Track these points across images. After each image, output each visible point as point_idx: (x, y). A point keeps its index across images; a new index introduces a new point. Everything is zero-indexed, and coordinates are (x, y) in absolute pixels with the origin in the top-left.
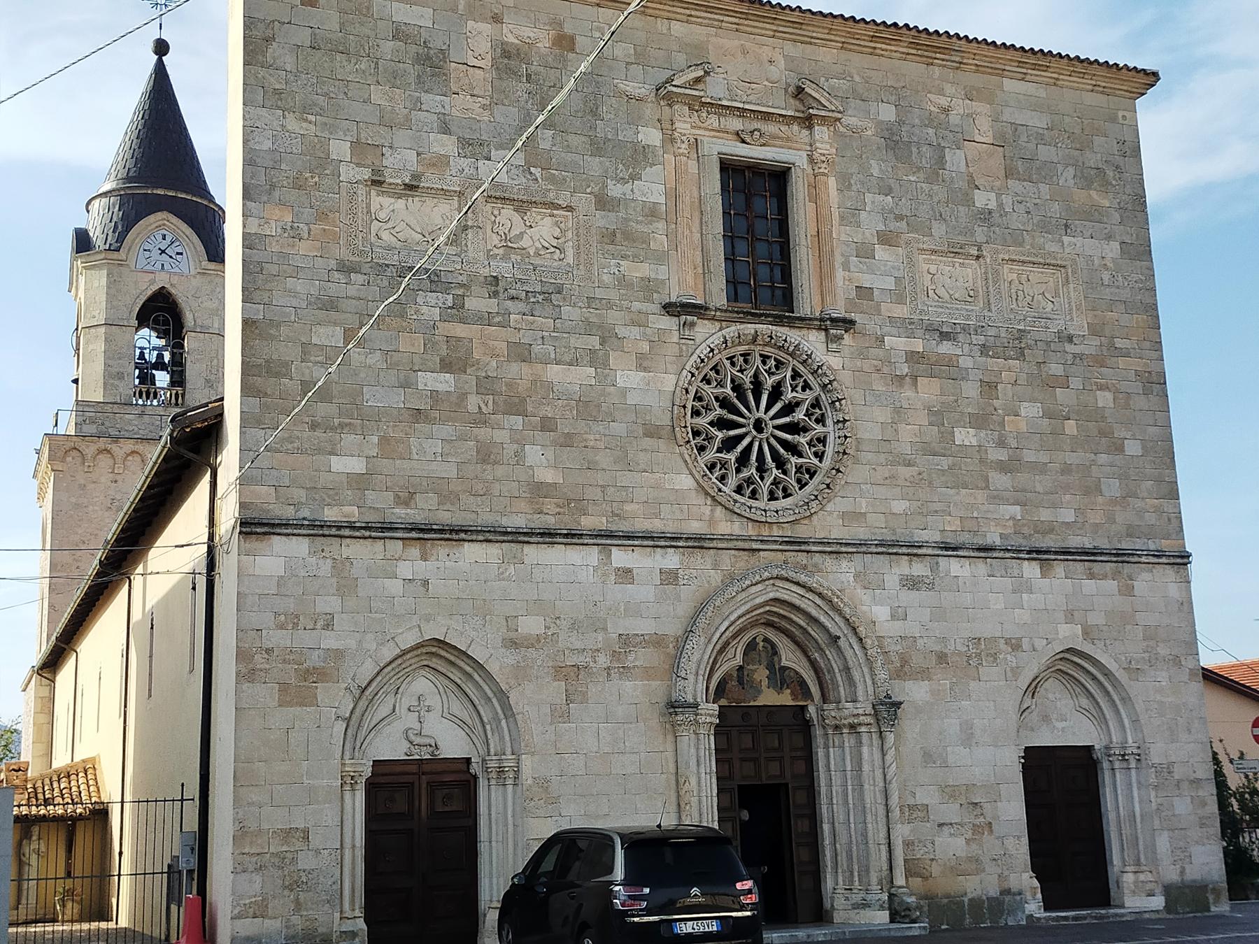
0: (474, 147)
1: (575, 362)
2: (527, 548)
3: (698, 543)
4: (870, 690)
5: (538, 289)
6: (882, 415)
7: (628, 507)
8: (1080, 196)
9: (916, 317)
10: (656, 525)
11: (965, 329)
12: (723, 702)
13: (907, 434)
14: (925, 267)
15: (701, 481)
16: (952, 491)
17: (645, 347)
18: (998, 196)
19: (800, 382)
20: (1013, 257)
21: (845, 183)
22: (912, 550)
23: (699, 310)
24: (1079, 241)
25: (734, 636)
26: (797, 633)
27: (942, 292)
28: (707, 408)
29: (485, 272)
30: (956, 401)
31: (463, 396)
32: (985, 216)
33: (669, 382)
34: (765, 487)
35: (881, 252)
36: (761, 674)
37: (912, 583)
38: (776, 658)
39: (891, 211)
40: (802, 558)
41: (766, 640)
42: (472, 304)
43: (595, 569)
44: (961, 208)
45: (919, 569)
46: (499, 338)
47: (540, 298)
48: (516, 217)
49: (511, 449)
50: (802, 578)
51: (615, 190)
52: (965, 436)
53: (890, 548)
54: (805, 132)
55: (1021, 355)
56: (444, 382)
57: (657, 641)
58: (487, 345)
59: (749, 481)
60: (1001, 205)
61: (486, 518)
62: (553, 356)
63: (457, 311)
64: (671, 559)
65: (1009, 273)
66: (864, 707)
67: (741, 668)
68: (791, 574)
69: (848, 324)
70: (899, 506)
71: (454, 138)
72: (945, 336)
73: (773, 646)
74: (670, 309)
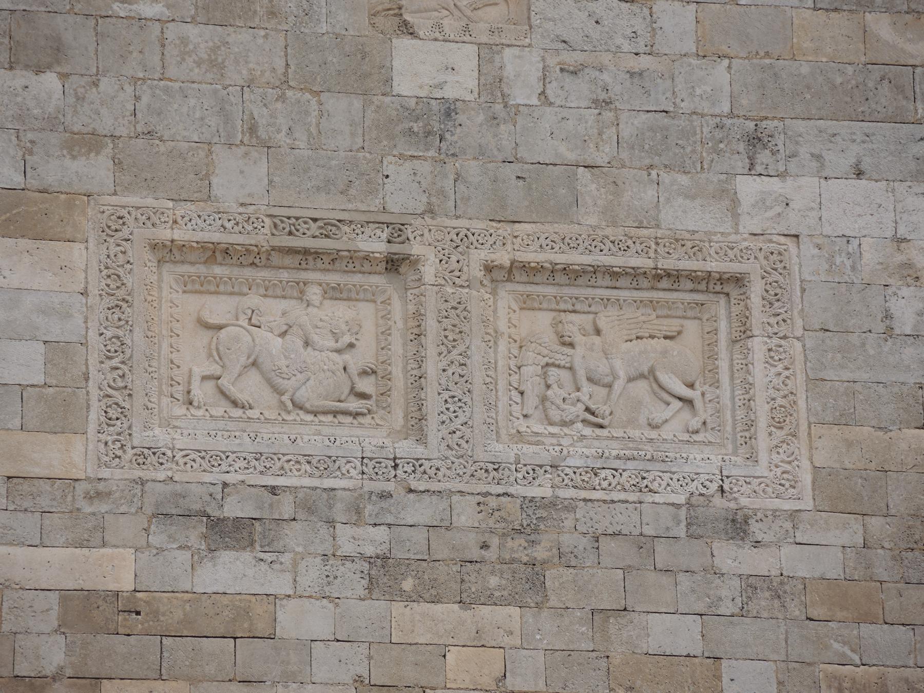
9: (115, 475)
11: (313, 506)
14: (192, 304)
18: (488, 52)
20: (531, 256)
24: (802, 189)
27: (250, 388)
32: (433, 123)
39: (52, 123)
44: (332, 102)
55: (530, 585)
60: (494, 86)
72: (227, 533)
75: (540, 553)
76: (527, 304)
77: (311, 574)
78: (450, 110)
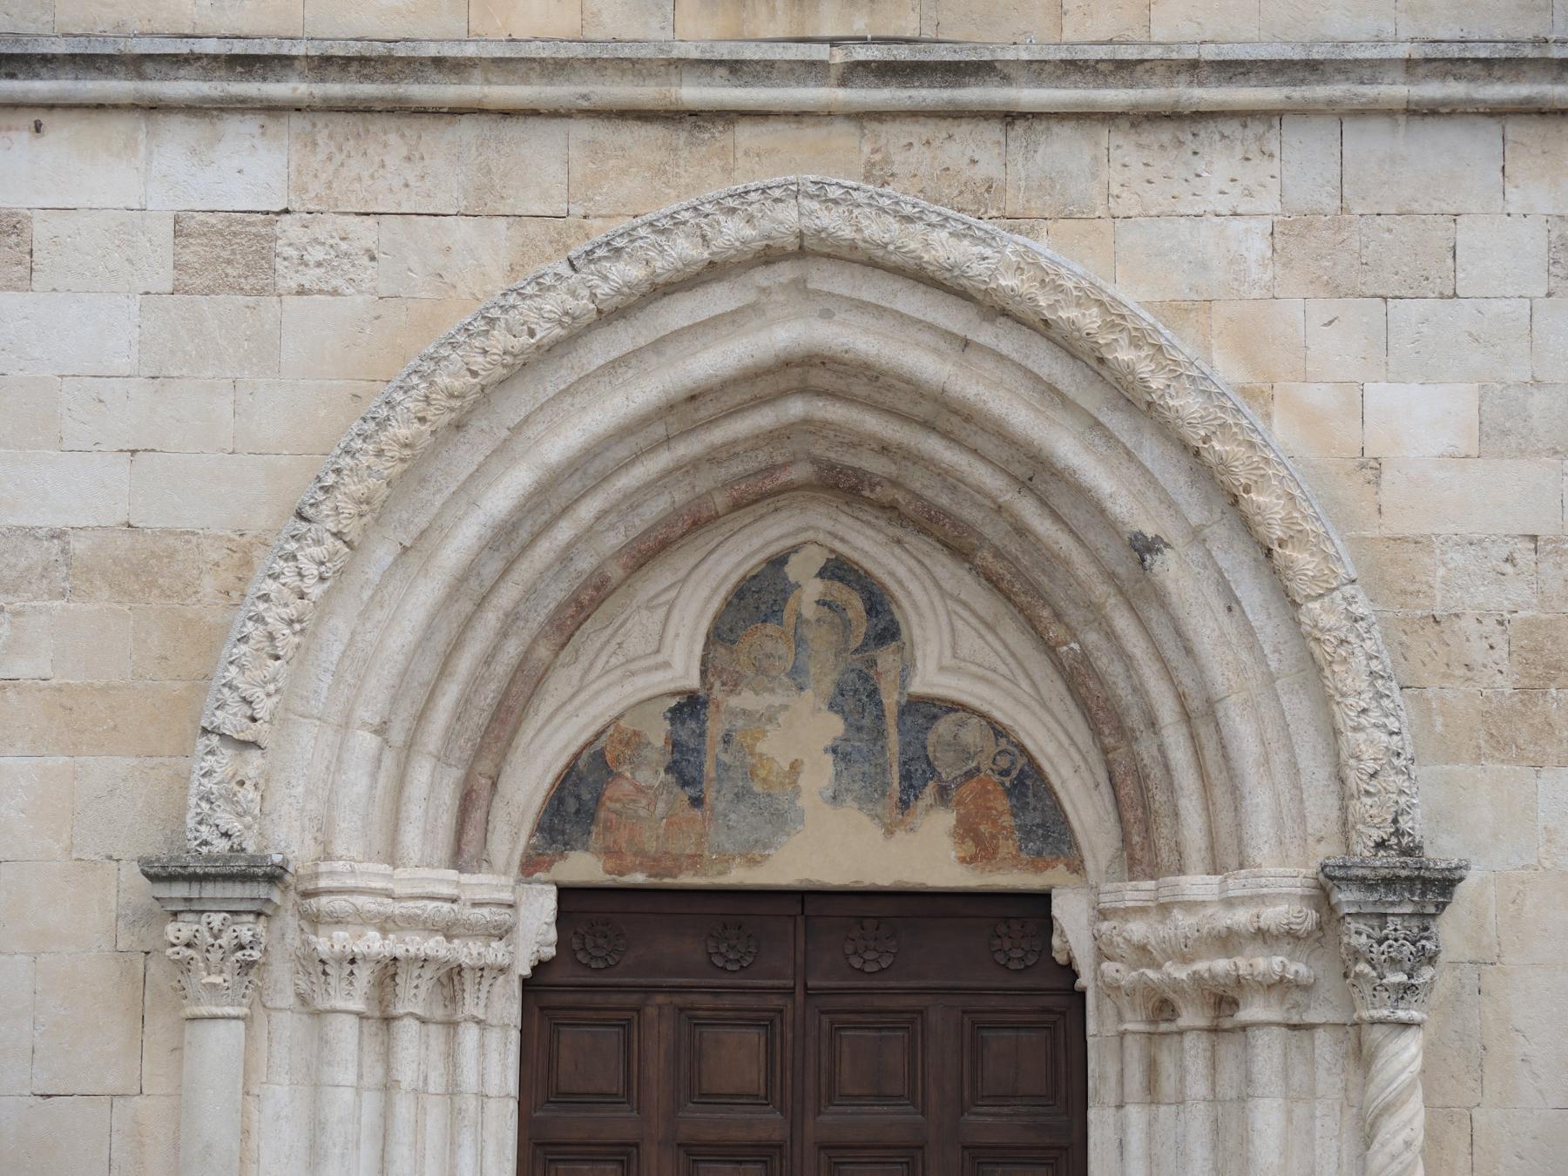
4: (1321, 809)
12: (584, 867)
25: (649, 552)
26: (994, 531)
36: (795, 731)
38: (886, 659)
40: (976, 153)
41: (839, 569)
50: (942, 248)
57: (139, 566)
64: (245, 169)
66: (1277, 886)
67: (689, 707)
68: (877, 230)
73: (877, 601)
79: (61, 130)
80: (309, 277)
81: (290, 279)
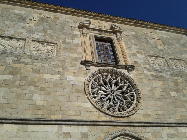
0: (30, 31)
1: (54, 74)
2: (29, 126)
3: (94, 123)
5: (44, 57)
6: (148, 88)
7: (69, 112)
8: (182, 49)
10: (79, 118)
11: (165, 71)
13: (157, 93)
15: (94, 104)
16: (175, 108)
17: (76, 71)
18: (163, 47)
19: (123, 82)
21: (126, 43)
22: (169, 125)
23: (91, 63)
27: (156, 64)
28: (96, 88)
29: (29, 54)
30: (168, 86)
31: (14, 81)
33: (84, 79)
34: (117, 108)
35: (138, 55)
37: (170, 136)
42: (22, 60)
43: (56, 133)
45: (172, 131)
46: (30, 68)
47: (44, 60)
48: (41, 46)
49: (28, 95)
51: (67, 41)
52: (173, 94)
53: (160, 125)
54: (115, 35)
55: (181, 76)
56: (9, 77)
58: (26, 70)
59: (111, 106)
61: (15, 116)
62: (47, 72)
63: (18, 61)
64: (85, 129)
65: (172, 62)
69: (133, 68)
70: (160, 112)
71: (25, 30)
72: (160, 72)
74: (83, 63)
75: (181, 74)
76: (172, 61)
77: (167, 75)
78: (163, 50)
79: (72, 126)
80: (90, 137)
81: (89, 137)
